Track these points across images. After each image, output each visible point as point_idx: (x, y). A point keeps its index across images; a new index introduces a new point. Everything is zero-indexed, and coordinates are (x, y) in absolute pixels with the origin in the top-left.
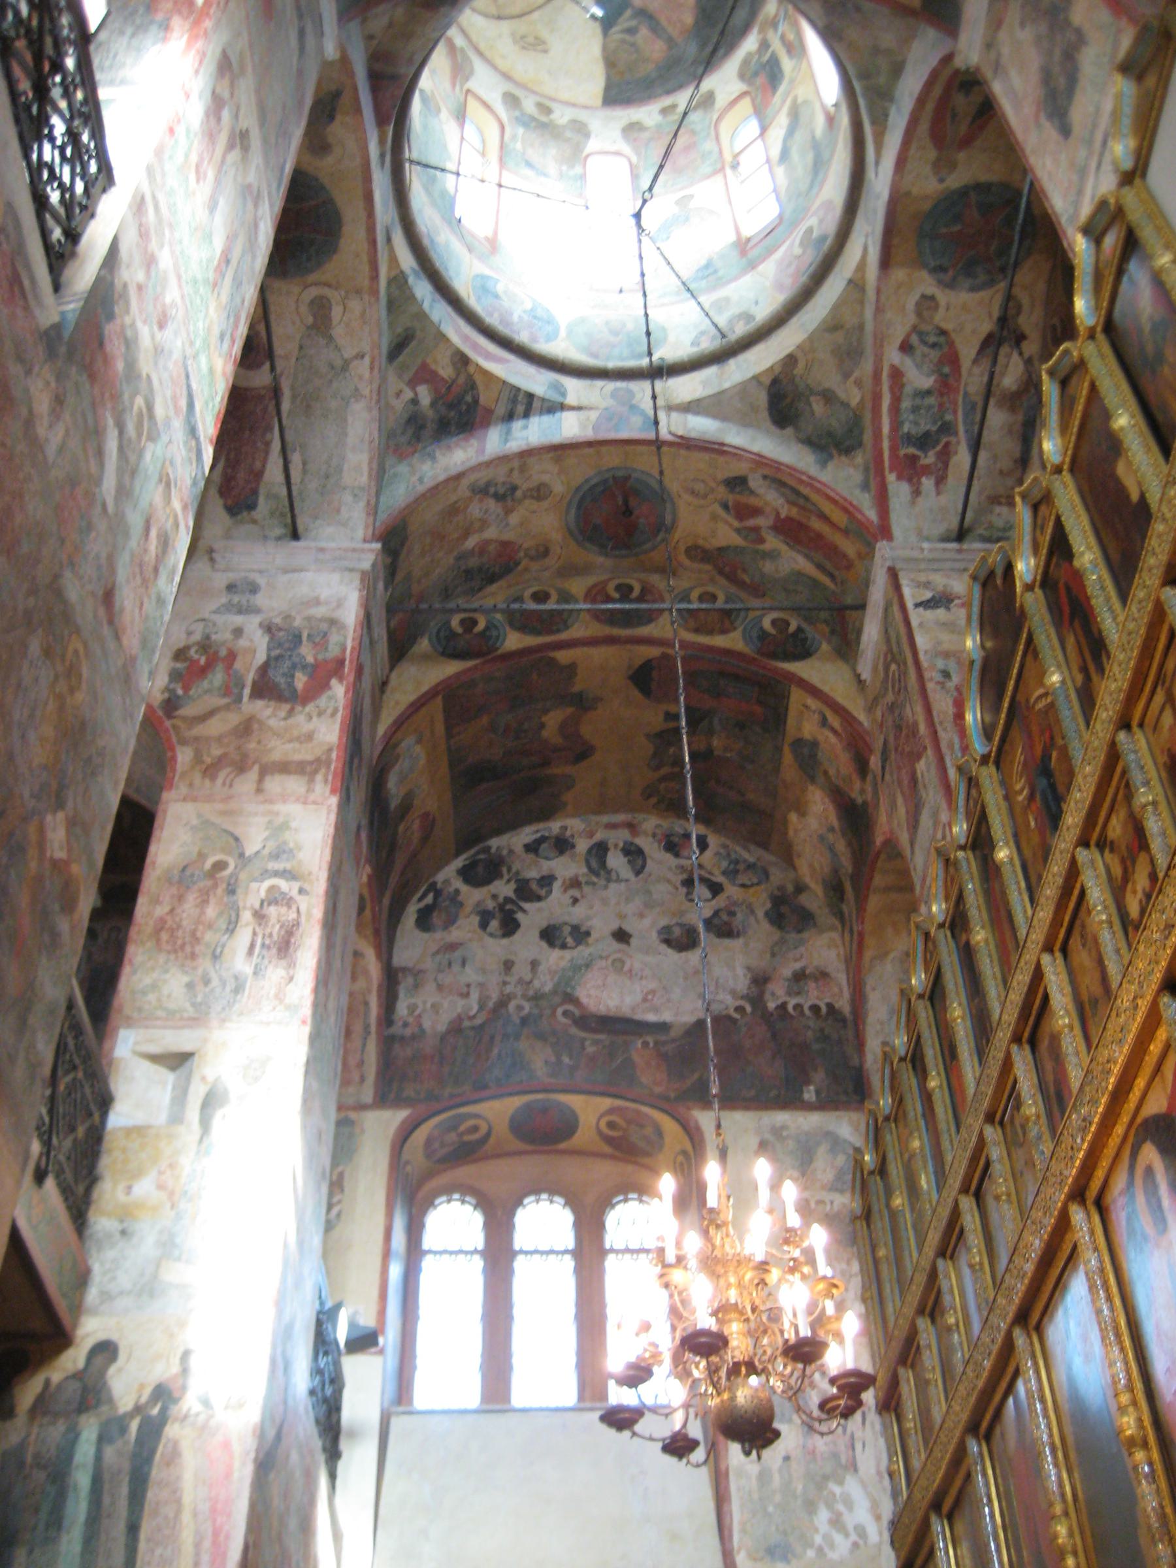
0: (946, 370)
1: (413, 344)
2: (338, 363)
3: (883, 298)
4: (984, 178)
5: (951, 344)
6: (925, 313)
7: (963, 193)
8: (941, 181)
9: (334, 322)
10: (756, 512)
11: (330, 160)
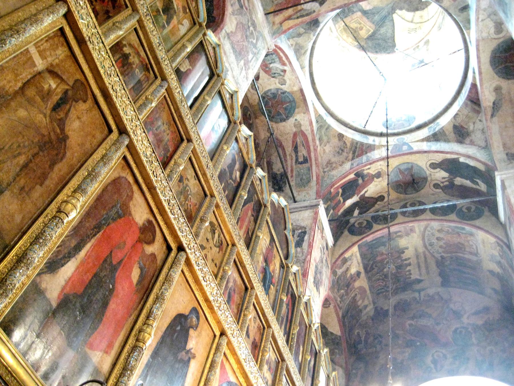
0: (267, 69)
2: (492, 17)
3: (298, 81)
4: (284, 124)
5: (269, 75)
6: (282, 80)
7: (288, 118)
8: (296, 120)
11: (494, 85)
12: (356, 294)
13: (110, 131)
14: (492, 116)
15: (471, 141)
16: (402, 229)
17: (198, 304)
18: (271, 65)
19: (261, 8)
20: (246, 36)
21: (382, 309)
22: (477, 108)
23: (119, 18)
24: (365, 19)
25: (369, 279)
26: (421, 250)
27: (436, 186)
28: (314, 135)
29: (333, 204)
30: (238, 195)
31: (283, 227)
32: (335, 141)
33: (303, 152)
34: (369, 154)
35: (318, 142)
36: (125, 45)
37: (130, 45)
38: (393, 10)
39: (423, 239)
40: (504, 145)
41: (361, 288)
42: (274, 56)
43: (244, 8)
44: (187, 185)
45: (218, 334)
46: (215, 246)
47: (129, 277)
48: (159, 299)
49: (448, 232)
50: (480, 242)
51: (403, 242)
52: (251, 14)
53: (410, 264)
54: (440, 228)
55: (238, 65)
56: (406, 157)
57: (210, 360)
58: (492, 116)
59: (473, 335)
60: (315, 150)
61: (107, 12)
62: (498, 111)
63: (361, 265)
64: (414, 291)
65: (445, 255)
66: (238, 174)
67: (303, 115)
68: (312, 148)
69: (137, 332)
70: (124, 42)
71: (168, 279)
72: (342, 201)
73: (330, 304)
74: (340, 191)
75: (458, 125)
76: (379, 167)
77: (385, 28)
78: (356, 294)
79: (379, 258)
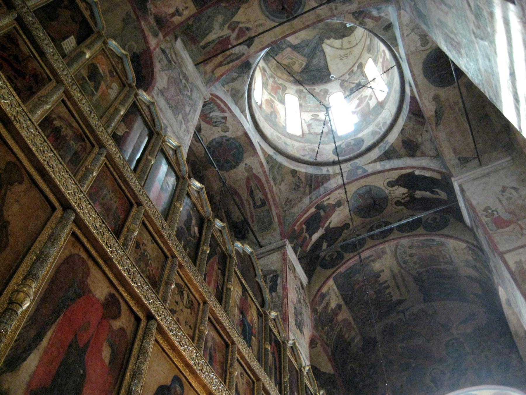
0: (208, 119)
1: (383, 27)
3: (240, 125)
5: (211, 125)
6: (224, 128)
7: (237, 164)
8: (246, 164)
9: (419, 41)
10: (238, 38)
11: (432, 95)
12: (341, 329)
13: (54, 209)
14: (437, 124)
15: (422, 153)
16: (374, 253)
18: (211, 115)
19: (190, 60)
20: (180, 90)
21: (370, 338)
22: (421, 120)
23: (43, 92)
24: (295, 54)
25: (351, 310)
26: (396, 270)
27: (398, 203)
28: (267, 176)
29: (299, 242)
30: (200, 251)
31: (252, 274)
32: (289, 178)
33: (259, 195)
34: (325, 185)
35: (272, 183)
36: (55, 119)
37: (61, 118)
38: (321, 40)
39: (396, 258)
40: (455, 151)
41: (344, 320)
42: (212, 105)
43: (173, 62)
44: (145, 250)
46: (186, 307)
48: (137, 374)
49: (419, 247)
50: (452, 250)
51: (377, 266)
52: (180, 67)
53: (388, 287)
54: (411, 244)
55: (176, 120)
56: (362, 180)
58: (437, 124)
59: (465, 345)
60: (271, 191)
61: (30, 88)
62: (441, 118)
63: (340, 297)
64: (398, 313)
65: (421, 270)
66: (196, 229)
67: (252, 158)
68: (267, 190)
70: (53, 116)
71: (142, 352)
72: (308, 236)
73: (317, 344)
74: (304, 226)
75: (406, 139)
76: (338, 196)
77: (317, 59)
78: (341, 329)
79: (356, 287)
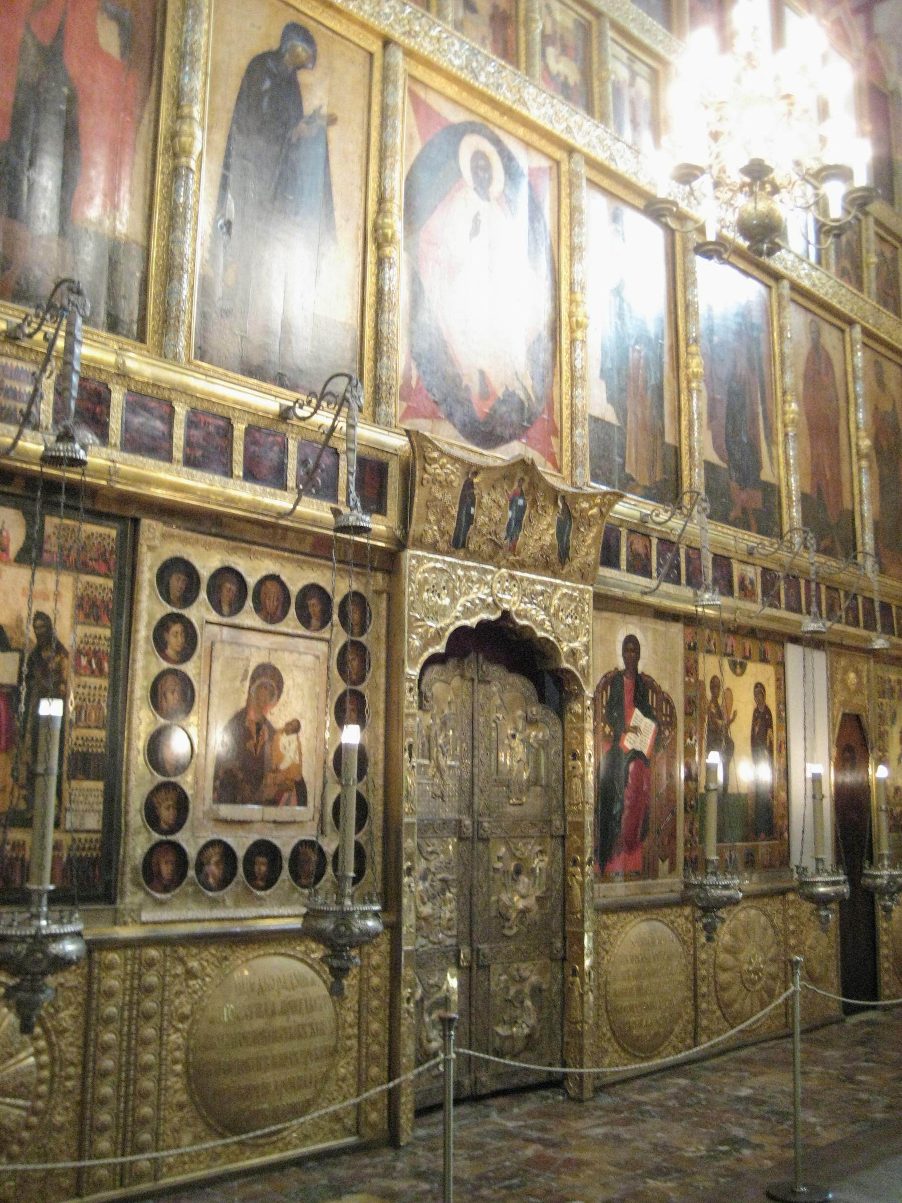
17: (295, 12)
45: (376, 47)
47: (96, 51)
48: (184, 56)
57: (376, 108)
69: (169, 142)
